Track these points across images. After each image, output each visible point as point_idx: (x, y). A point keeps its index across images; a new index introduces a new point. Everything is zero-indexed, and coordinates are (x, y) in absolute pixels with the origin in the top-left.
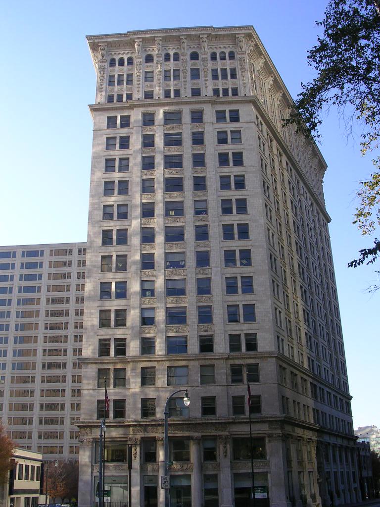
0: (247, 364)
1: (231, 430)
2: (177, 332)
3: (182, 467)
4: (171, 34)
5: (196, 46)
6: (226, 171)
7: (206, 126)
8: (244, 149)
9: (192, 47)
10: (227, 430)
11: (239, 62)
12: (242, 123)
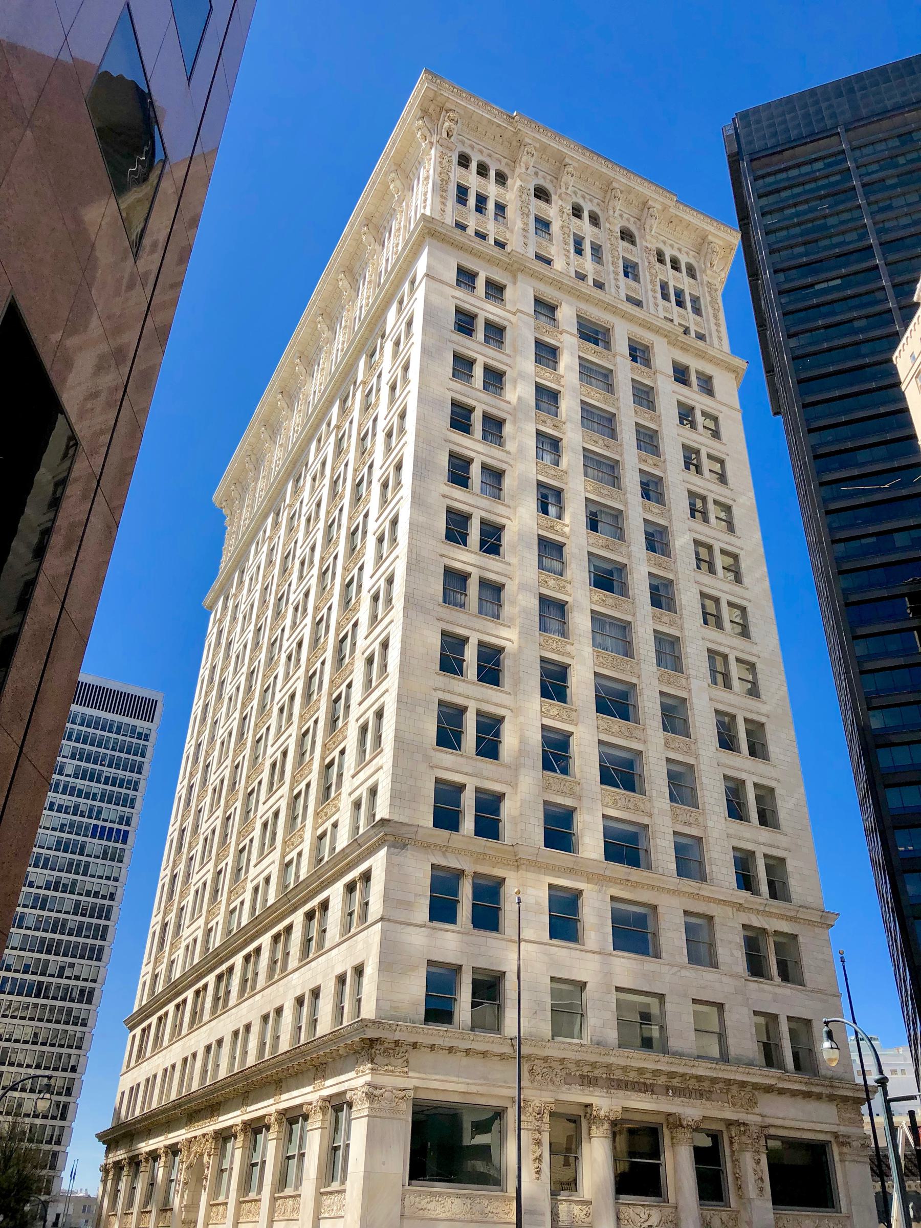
0: (775, 931)
1: (767, 1111)
4: (599, 168)
5: (632, 219)
7: (660, 378)
8: (728, 455)
9: (625, 216)
10: (756, 1110)
11: (706, 289)
12: (721, 403)
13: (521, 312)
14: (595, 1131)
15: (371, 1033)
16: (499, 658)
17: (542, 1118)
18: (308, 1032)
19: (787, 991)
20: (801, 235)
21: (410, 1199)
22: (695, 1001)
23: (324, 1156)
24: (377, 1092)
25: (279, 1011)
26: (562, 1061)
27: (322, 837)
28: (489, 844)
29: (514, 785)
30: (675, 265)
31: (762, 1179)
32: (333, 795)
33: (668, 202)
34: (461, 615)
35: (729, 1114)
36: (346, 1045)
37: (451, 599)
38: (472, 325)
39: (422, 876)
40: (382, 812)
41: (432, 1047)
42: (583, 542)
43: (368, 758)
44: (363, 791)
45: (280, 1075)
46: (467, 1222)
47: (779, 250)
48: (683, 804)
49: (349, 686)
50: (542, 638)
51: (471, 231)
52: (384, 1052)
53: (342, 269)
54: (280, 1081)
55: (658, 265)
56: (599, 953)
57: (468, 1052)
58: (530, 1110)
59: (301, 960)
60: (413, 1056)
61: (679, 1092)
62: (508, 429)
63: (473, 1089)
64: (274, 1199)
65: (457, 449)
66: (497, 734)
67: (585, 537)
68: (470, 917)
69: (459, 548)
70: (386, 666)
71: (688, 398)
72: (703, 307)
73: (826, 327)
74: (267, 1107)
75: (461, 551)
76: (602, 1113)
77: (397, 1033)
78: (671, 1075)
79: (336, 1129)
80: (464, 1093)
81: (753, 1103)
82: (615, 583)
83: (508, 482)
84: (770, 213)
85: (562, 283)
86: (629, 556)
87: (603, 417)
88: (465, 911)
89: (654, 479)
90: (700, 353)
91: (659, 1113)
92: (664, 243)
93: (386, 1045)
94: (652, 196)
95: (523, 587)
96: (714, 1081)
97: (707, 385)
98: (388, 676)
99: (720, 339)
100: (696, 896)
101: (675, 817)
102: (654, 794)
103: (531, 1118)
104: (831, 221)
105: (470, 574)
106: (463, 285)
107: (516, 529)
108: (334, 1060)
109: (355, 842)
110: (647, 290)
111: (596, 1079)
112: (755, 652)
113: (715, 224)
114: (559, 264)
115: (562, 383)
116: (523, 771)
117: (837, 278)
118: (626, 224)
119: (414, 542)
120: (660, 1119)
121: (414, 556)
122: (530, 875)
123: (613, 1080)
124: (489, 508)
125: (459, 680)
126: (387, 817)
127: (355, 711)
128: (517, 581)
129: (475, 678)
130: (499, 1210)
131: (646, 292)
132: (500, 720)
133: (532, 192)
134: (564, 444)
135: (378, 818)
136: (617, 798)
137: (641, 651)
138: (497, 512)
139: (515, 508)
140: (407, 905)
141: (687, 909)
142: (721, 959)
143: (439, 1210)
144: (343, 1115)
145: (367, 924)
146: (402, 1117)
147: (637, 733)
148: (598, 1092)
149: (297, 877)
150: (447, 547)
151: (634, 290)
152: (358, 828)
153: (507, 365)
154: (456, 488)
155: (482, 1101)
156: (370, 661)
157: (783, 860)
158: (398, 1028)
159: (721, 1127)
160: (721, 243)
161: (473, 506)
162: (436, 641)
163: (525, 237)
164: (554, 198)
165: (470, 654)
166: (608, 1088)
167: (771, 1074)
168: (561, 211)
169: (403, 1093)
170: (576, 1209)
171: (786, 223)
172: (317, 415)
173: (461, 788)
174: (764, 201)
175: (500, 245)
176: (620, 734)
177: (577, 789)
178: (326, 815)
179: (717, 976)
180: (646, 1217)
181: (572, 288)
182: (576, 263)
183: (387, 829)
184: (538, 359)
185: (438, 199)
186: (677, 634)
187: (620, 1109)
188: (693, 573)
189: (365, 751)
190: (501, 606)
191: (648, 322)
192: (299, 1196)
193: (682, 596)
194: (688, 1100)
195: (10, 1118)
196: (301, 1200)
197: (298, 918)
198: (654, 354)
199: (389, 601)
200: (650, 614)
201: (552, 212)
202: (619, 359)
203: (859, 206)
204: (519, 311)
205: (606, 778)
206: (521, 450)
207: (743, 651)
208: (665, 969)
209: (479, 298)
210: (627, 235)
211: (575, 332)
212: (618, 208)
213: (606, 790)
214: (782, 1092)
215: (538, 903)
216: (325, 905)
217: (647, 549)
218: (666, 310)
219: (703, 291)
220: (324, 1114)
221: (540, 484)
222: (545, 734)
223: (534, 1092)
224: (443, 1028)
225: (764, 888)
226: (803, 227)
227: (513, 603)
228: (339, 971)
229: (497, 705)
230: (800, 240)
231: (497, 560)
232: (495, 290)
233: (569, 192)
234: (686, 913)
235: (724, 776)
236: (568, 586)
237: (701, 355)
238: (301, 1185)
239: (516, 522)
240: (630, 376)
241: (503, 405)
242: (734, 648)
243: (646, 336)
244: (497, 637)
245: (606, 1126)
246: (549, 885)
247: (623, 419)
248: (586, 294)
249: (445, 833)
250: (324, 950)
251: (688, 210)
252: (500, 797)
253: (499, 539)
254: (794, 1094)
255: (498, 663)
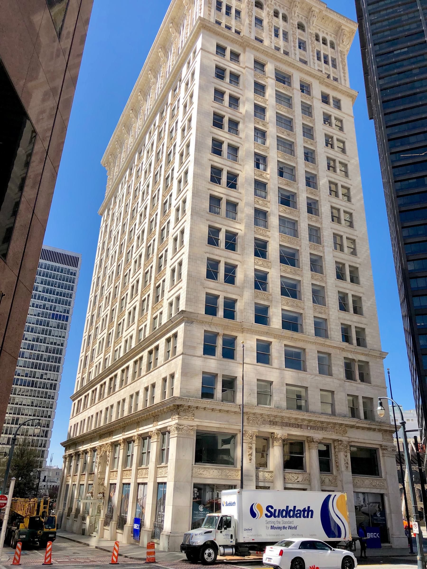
2: (292, 306)
3: (298, 477)
5: (304, 18)
6: (332, 153)
7: (315, 101)
9: (300, 16)
10: (347, 435)
11: (339, 54)
12: (344, 113)
13: (248, 67)
14: (275, 443)
15: (178, 403)
16: (235, 238)
17: (252, 438)
18: (150, 401)
19: (363, 386)
20: (389, 25)
21: (195, 470)
22: (321, 390)
23: (158, 453)
24: (181, 427)
25: (137, 393)
26: (262, 415)
27: (155, 318)
28: (230, 322)
29: (241, 296)
30: (325, 42)
31: (347, 463)
32: (160, 300)
33: (322, 8)
34: (218, 218)
35: (335, 437)
36: (167, 408)
37: (213, 210)
38: (224, 74)
39: (200, 335)
40: (182, 307)
41: (205, 409)
42: (276, 182)
43: (175, 283)
44: (174, 298)
45: (139, 420)
46: (220, 479)
47: (377, 33)
48: (319, 304)
49: (166, 251)
50: (255, 229)
51: (223, 25)
52: (184, 410)
53: (160, 46)
54: (139, 422)
55: (316, 42)
56: (279, 369)
57: (220, 411)
58: (247, 435)
59: (147, 371)
60: (196, 412)
61: (312, 428)
62: (240, 126)
63: (222, 426)
64: (137, 470)
65: (216, 137)
66: (234, 273)
67: (277, 179)
68: (221, 353)
69: (217, 185)
70: (183, 242)
71: (328, 111)
72: (337, 64)
73: (399, 73)
74: (133, 433)
75: (218, 187)
76: (279, 436)
77: (189, 402)
78: (310, 421)
79: (163, 442)
80: (219, 427)
81: (345, 432)
82: (291, 202)
83: (240, 153)
84: (374, 13)
85: (268, 52)
86: (298, 189)
87: (287, 121)
88: (219, 350)
89: (310, 151)
90: (335, 88)
91: (303, 436)
92: (319, 30)
93: (184, 407)
94: (314, 5)
95: (247, 204)
96: (328, 423)
97: (338, 104)
98: (184, 246)
99: (345, 80)
100: (323, 345)
101: (315, 310)
102: (306, 299)
103: (248, 438)
104: (404, 18)
105: (222, 198)
106: (219, 54)
107: (244, 176)
108: (162, 414)
109: (170, 321)
110: (310, 56)
111: (276, 422)
112: (355, 234)
113: (345, 20)
114: (266, 42)
115: (267, 103)
116: (245, 290)
117: (405, 48)
118: (300, 20)
119: (196, 183)
120: (304, 439)
121: (196, 190)
122: (248, 335)
123: (284, 423)
124: (231, 166)
125: (217, 248)
126: (184, 309)
127: (169, 263)
128: (244, 201)
129: (224, 247)
130: (234, 475)
131: (309, 56)
132: (235, 267)
133: (254, 4)
134: (268, 134)
135: (180, 310)
136: (288, 301)
137: (302, 234)
138: (236, 168)
139: (244, 166)
140: (194, 348)
141: (319, 350)
142: (333, 372)
143: (208, 474)
144: (166, 436)
145: (176, 356)
146: (191, 437)
147: (298, 272)
148: (277, 427)
149: (144, 336)
150: (211, 185)
151: (304, 56)
152: (171, 314)
153: (240, 94)
154: (215, 156)
155: (226, 431)
156: (176, 239)
157: (364, 329)
158: (190, 400)
159: (331, 442)
160: (348, 29)
161: (224, 165)
162: (206, 230)
163: (250, 28)
164: (265, 6)
165: (222, 237)
166: (281, 426)
167: (354, 420)
168: (268, 14)
169: (192, 428)
170: (266, 475)
171: (382, 19)
172: (149, 120)
173: (217, 297)
174: (370, 7)
175: (238, 32)
176: (290, 273)
177: (270, 297)
178: (157, 309)
179: (331, 380)
180: (296, 478)
181: (273, 55)
182: (275, 42)
183: (184, 315)
184: (256, 91)
185: (207, 8)
186: (319, 226)
187: (286, 435)
188: (328, 197)
189: (174, 281)
190: (236, 213)
191: (310, 72)
192: (148, 468)
193: (322, 208)
194: (316, 431)
195: (23, 437)
196: (149, 470)
197: (145, 353)
198: (312, 88)
199: (184, 211)
200: (307, 217)
201: (264, 14)
202: (295, 91)
203: (418, 10)
204: (246, 67)
205: (284, 292)
206: (247, 137)
207: (350, 234)
208: (308, 376)
209: (228, 61)
210: (300, 26)
211: (274, 77)
212: (297, 11)
213: (283, 298)
214: (358, 428)
215: (251, 347)
216: (157, 348)
217: (306, 185)
218: (319, 66)
219: (338, 55)
220: (158, 436)
221: (256, 154)
222: (256, 273)
223: (249, 427)
224: (209, 400)
225: (355, 341)
226: (390, 21)
227: (242, 212)
228: (163, 376)
229: (234, 260)
230: (388, 27)
231: (235, 191)
232: (235, 56)
233: (272, 3)
234: (319, 352)
235: (338, 291)
236: (268, 204)
237: (335, 89)
238: (149, 464)
239: (244, 172)
240: (300, 99)
241: (238, 114)
242: (346, 233)
243: (308, 79)
244: (234, 228)
245: (280, 441)
246: (257, 339)
247: (296, 121)
248: (280, 58)
249: (210, 317)
250: (157, 367)
251: (332, 12)
252: (235, 301)
253: (236, 181)
254: (363, 428)
255: (235, 241)
